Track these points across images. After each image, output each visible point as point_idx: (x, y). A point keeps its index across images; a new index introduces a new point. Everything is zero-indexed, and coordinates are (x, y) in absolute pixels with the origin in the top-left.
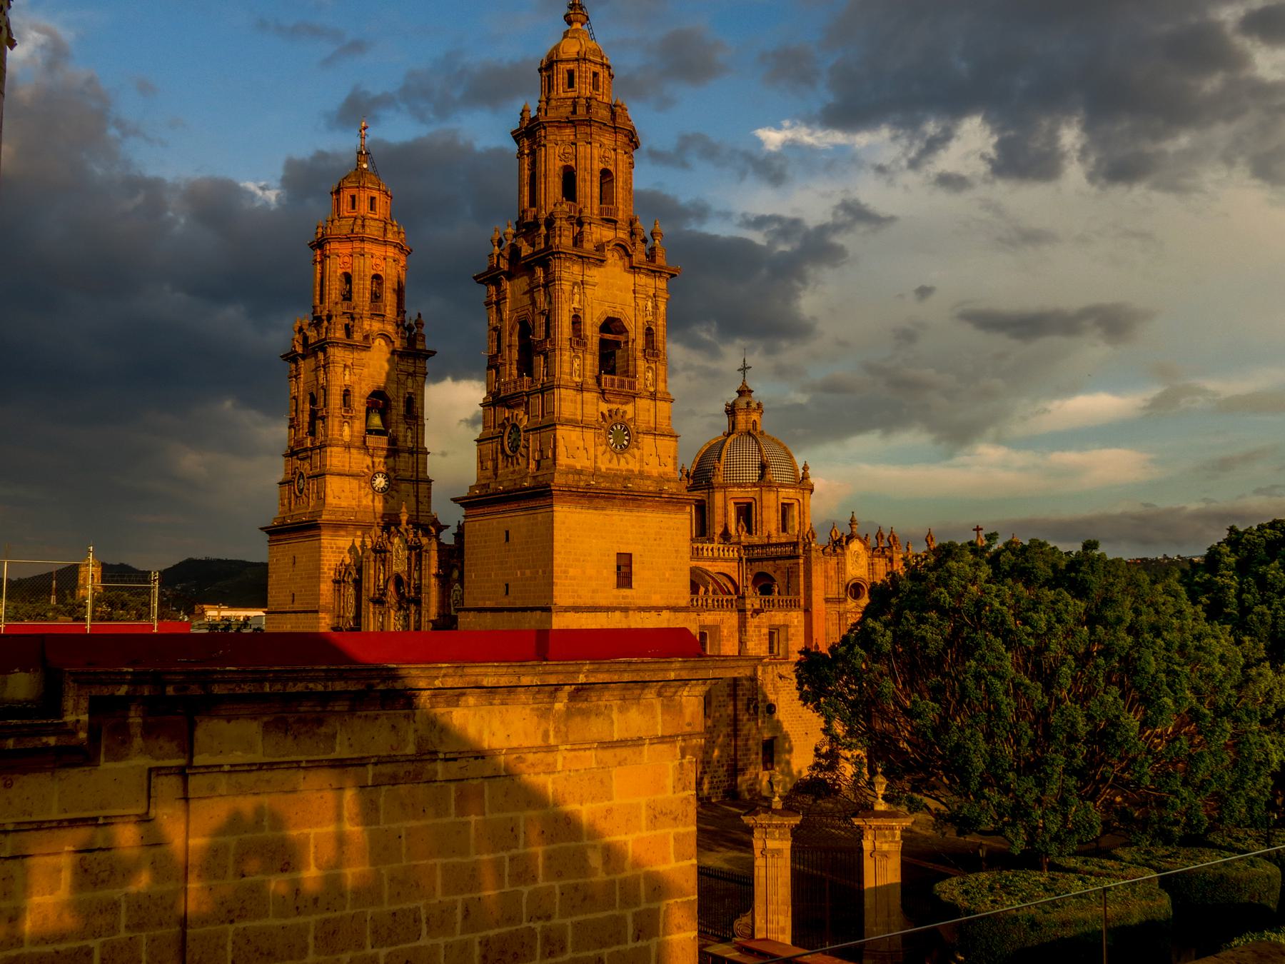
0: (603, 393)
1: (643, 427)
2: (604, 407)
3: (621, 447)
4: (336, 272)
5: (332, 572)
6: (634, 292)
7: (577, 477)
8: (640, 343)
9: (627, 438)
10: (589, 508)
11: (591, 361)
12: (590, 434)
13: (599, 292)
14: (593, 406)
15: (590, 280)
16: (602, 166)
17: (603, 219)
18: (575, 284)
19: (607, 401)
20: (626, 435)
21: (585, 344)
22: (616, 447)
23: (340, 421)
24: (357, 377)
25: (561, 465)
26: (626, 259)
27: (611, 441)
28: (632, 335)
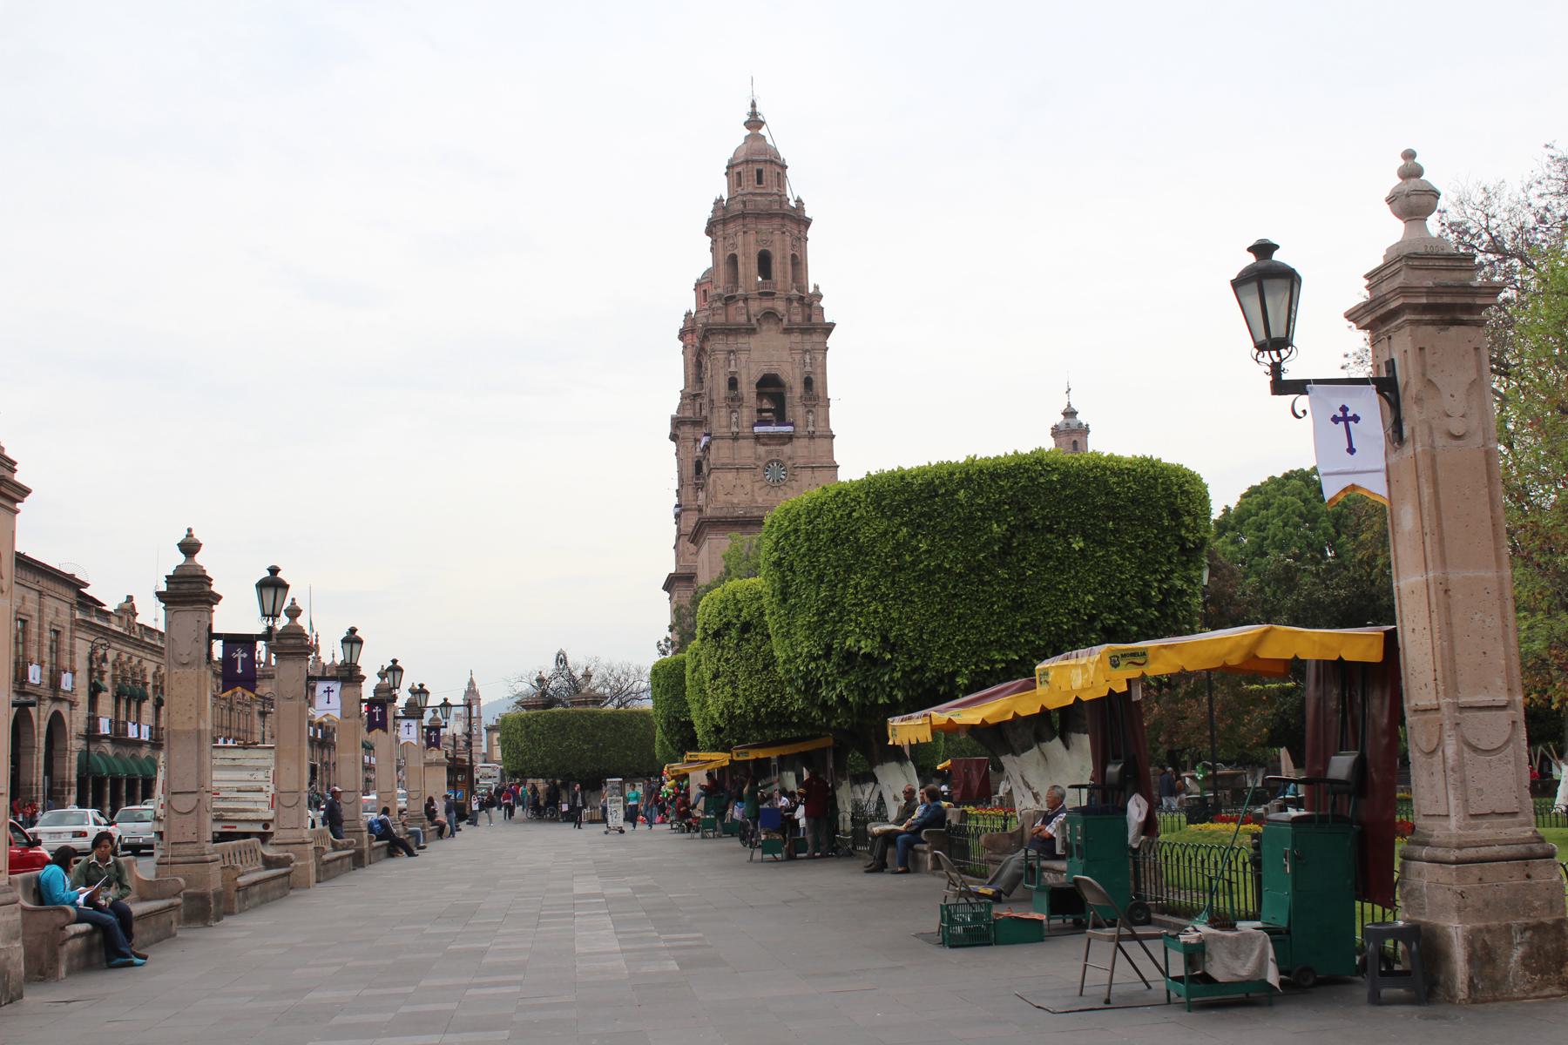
1: (800, 462)
2: (761, 450)
6: (791, 349)
8: (798, 389)
11: (747, 414)
12: (746, 477)
13: (755, 355)
14: (746, 451)
17: (760, 294)
18: (730, 352)
19: (764, 445)
21: (741, 399)
27: (768, 477)
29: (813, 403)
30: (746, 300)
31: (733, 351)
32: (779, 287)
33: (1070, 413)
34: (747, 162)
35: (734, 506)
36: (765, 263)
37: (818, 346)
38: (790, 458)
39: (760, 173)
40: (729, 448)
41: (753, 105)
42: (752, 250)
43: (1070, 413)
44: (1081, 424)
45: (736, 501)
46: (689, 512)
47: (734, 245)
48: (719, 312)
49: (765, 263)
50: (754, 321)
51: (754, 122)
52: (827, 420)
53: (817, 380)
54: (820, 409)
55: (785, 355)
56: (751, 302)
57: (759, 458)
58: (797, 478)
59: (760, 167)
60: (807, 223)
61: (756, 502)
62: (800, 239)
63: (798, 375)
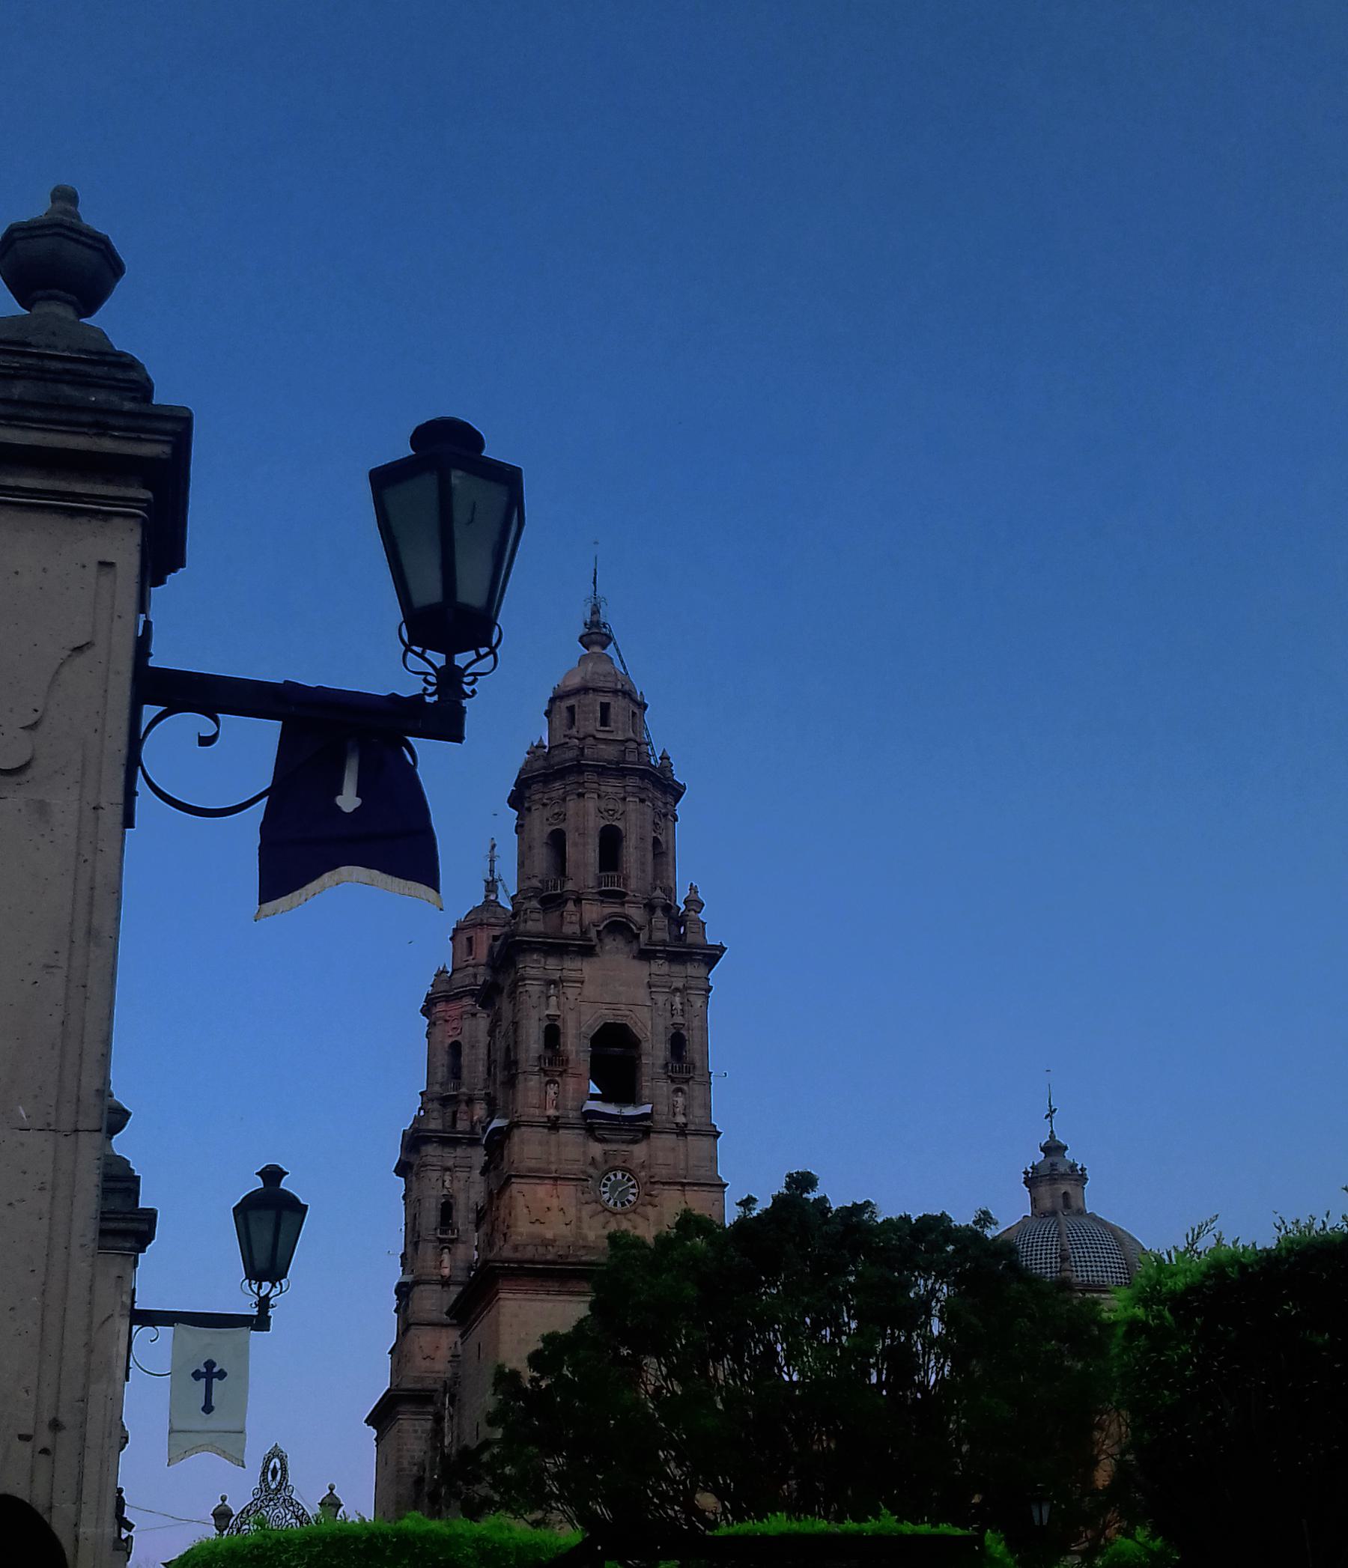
0: (591, 1131)
1: (662, 1173)
2: (596, 1149)
3: (623, 1204)
4: (442, 1042)
5: (416, 1468)
7: (541, 1250)
9: (633, 1190)
10: (559, 1293)
12: (568, 1190)
13: (589, 990)
15: (573, 974)
16: (603, 823)
17: (601, 893)
20: (633, 1186)
22: (615, 1204)
23: (435, 1248)
24: (462, 1182)
25: (521, 1234)
26: (634, 942)
27: (606, 1196)
28: (646, 1046)
29: (688, 1076)
30: (578, 901)
31: (554, 982)
32: (633, 884)
33: (1053, 1149)
34: (584, 690)
35: (547, 1243)
36: (611, 842)
37: (693, 983)
38: (643, 1166)
39: (605, 708)
40: (540, 1144)
41: (595, 611)
42: (591, 824)
43: (1053, 1149)
44: (1073, 1166)
45: (549, 1235)
46: (427, 1287)
47: (561, 816)
48: (535, 916)
49: (611, 842)
50: (593, 934)
51: (596, 635)
52: (707, 1107)
53: (693, 1038)
54: (696, 1087)
55: (642, 995)
56: (586, 906)
57: (593, 1162)
58: (656, 1201)
59: (606, 700)
60: (676, 792)
61: (585, 1238)
62: (665, 815)
63: (661, 1029)
